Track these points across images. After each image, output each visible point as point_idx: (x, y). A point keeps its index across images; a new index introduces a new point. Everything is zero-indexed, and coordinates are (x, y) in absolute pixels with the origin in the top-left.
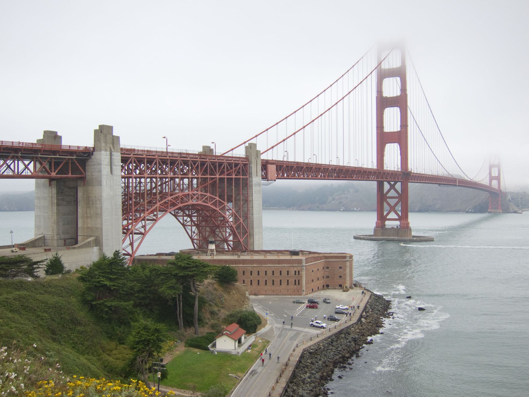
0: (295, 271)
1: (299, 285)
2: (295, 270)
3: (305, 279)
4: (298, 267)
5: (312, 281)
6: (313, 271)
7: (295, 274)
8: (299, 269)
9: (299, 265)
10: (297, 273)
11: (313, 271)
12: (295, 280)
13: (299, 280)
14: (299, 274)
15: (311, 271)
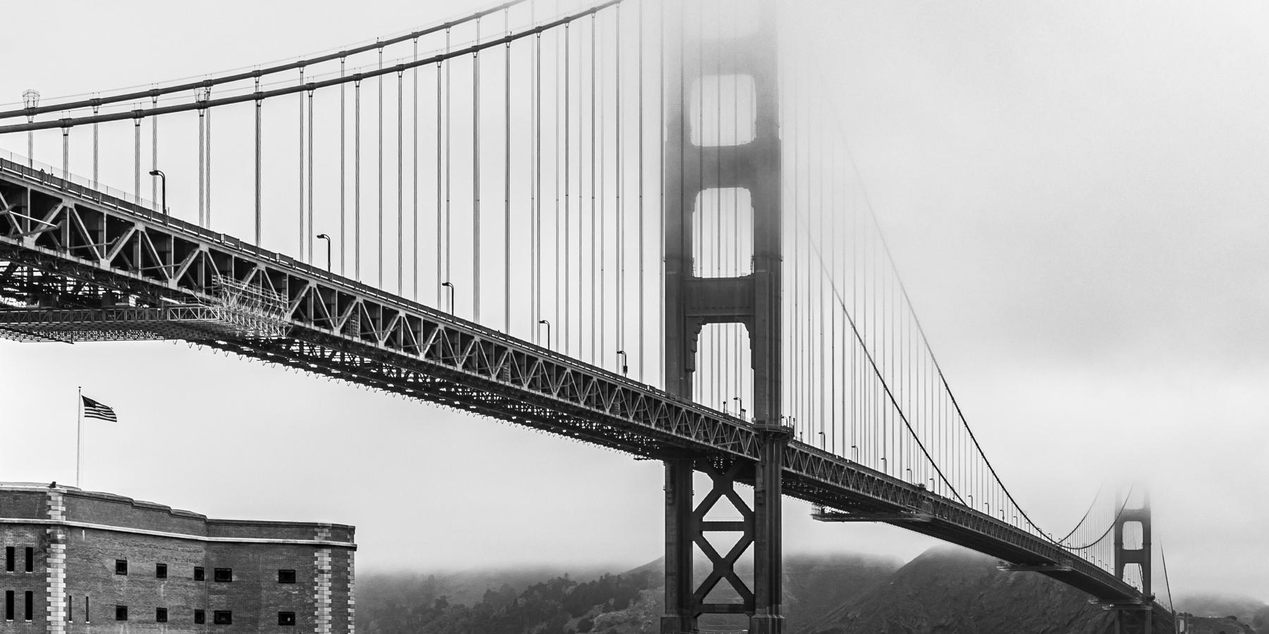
0: (10, 551)
1: (29, 616)
2: (10, 543)
3: (65, 590)
4: (21, 530)
5: (114, 616)
6: (121, 567)
7: (10, 566)
8: (30, 539)
9: (31, 520)
10: (20, 561)
11: (121, 567)
12: (10, 595)
13: (29, 595)
14: (29, 567)
15: (111, 564)
